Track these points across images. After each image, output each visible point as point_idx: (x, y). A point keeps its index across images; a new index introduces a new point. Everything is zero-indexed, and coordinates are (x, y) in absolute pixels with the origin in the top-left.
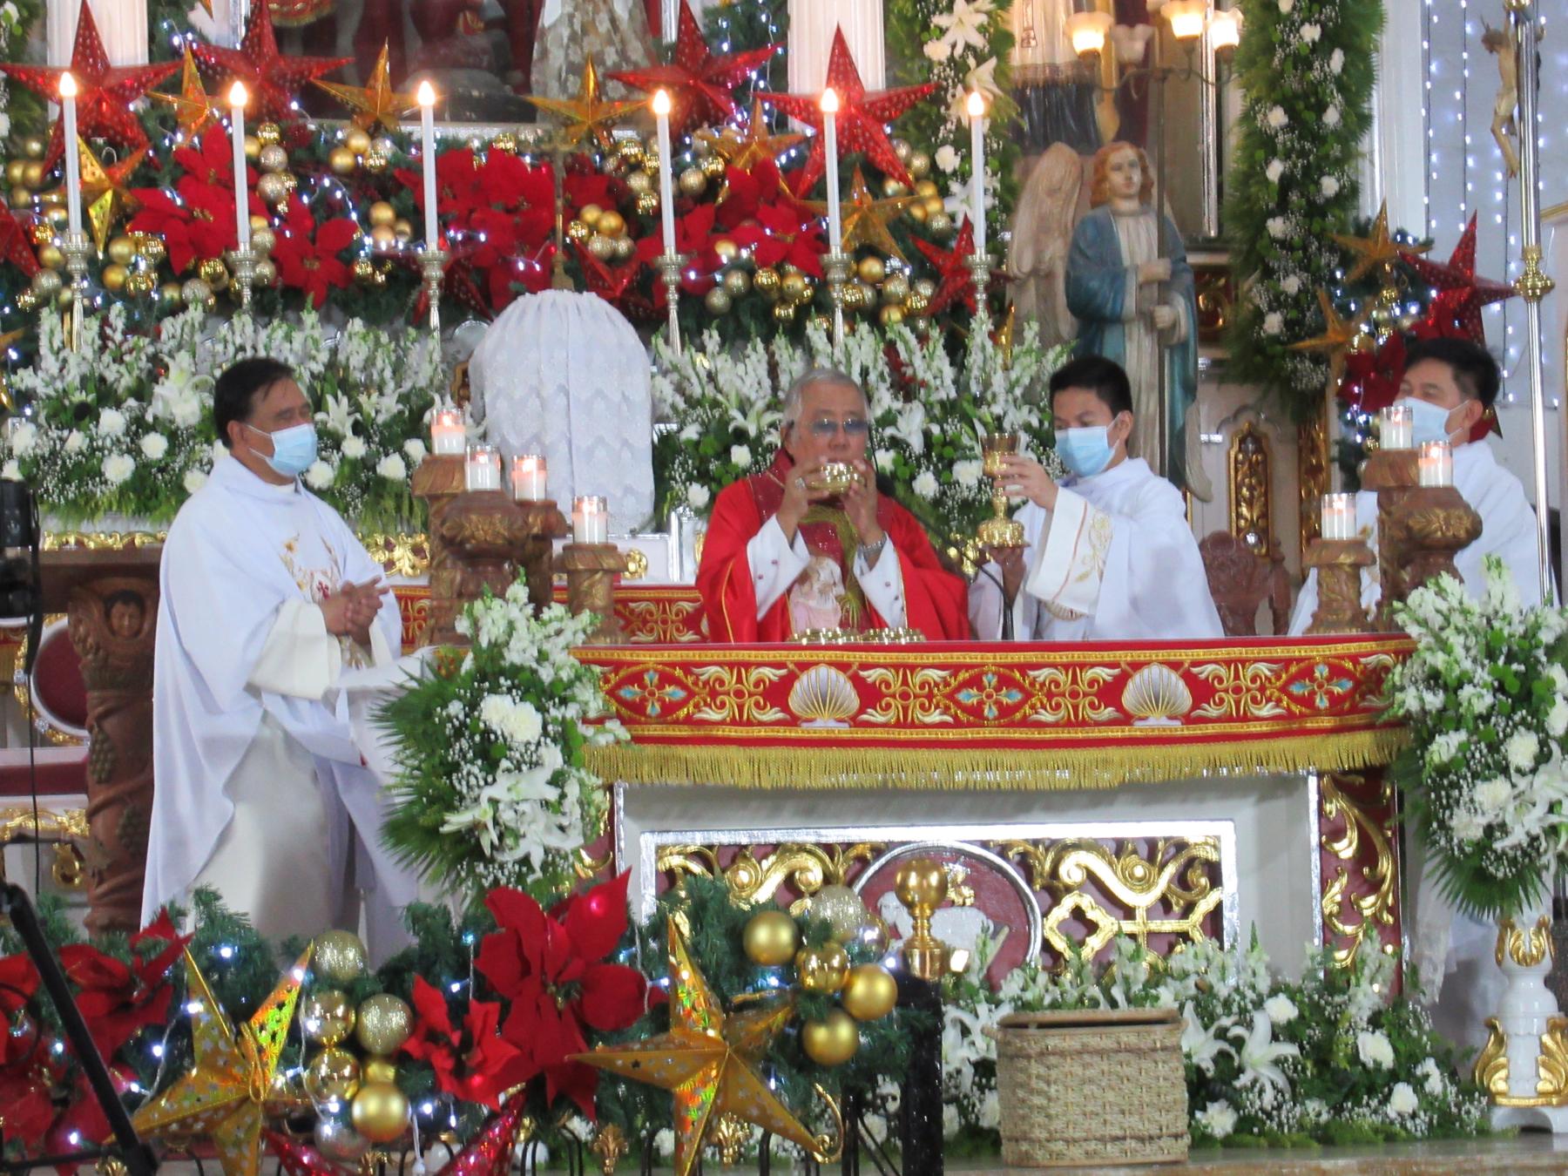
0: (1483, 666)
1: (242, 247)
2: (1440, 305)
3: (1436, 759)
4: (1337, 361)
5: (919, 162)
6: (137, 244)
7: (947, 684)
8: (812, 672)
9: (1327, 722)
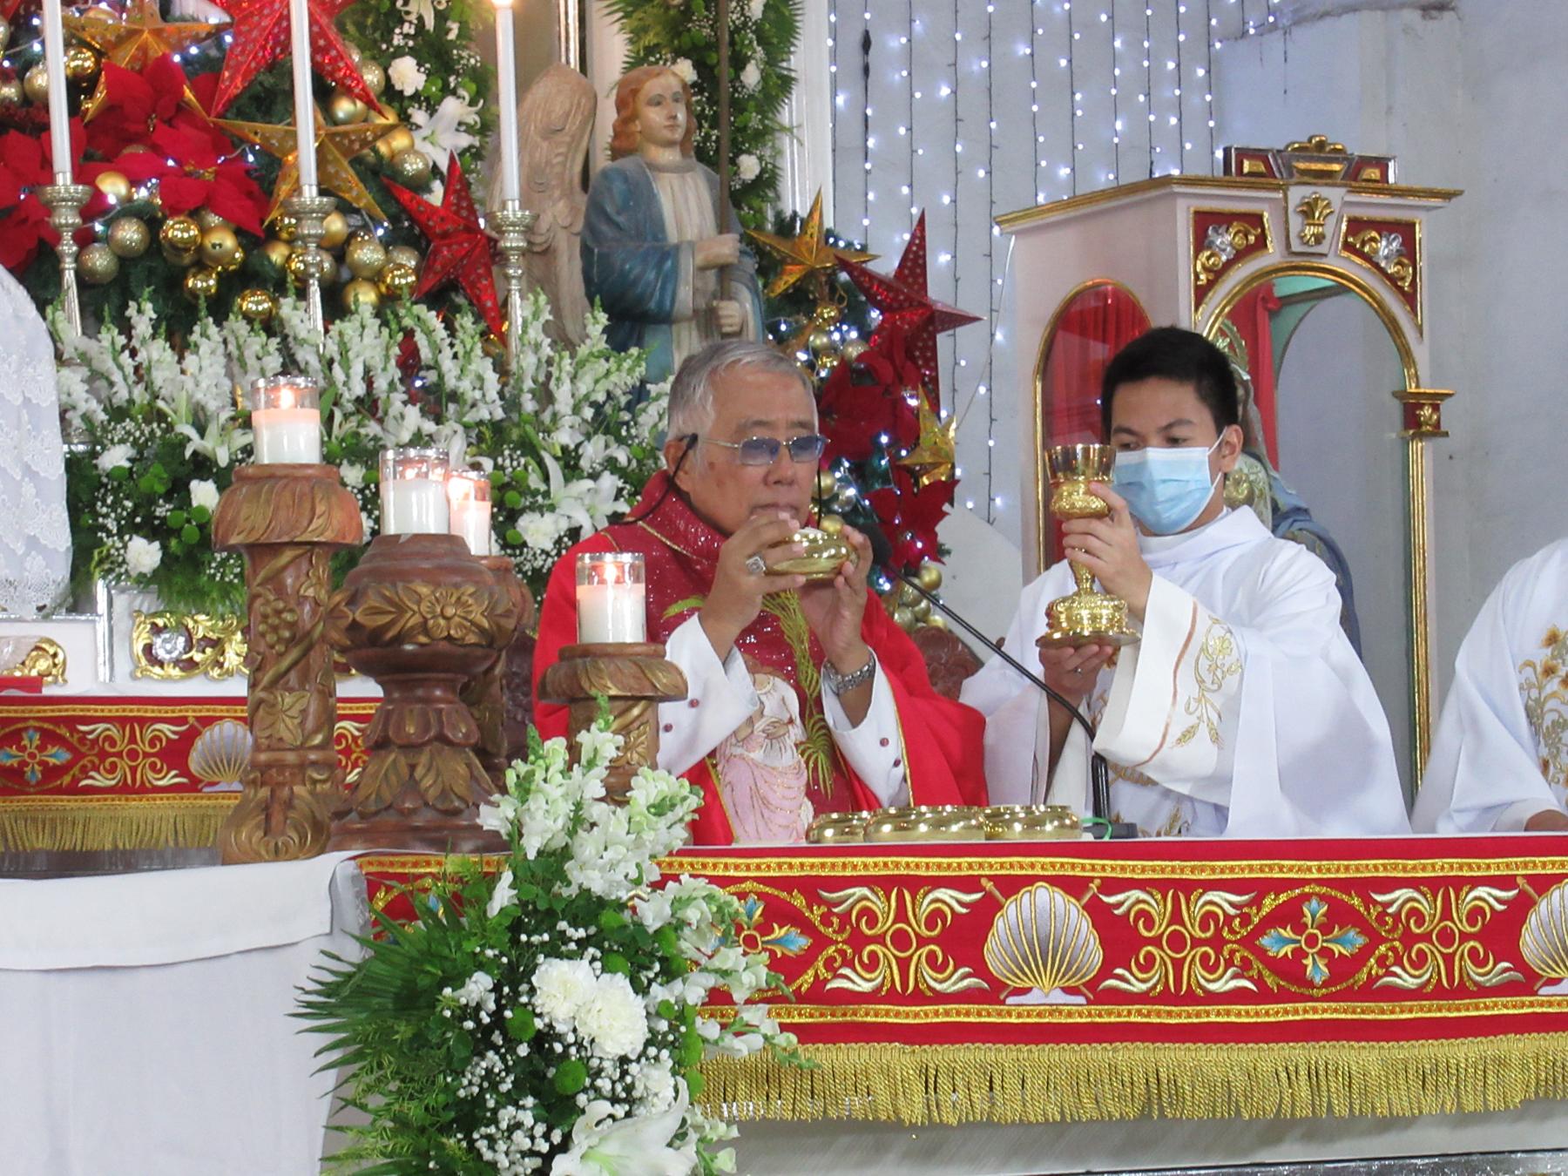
5: (372, 77)
8: (1024, 896)
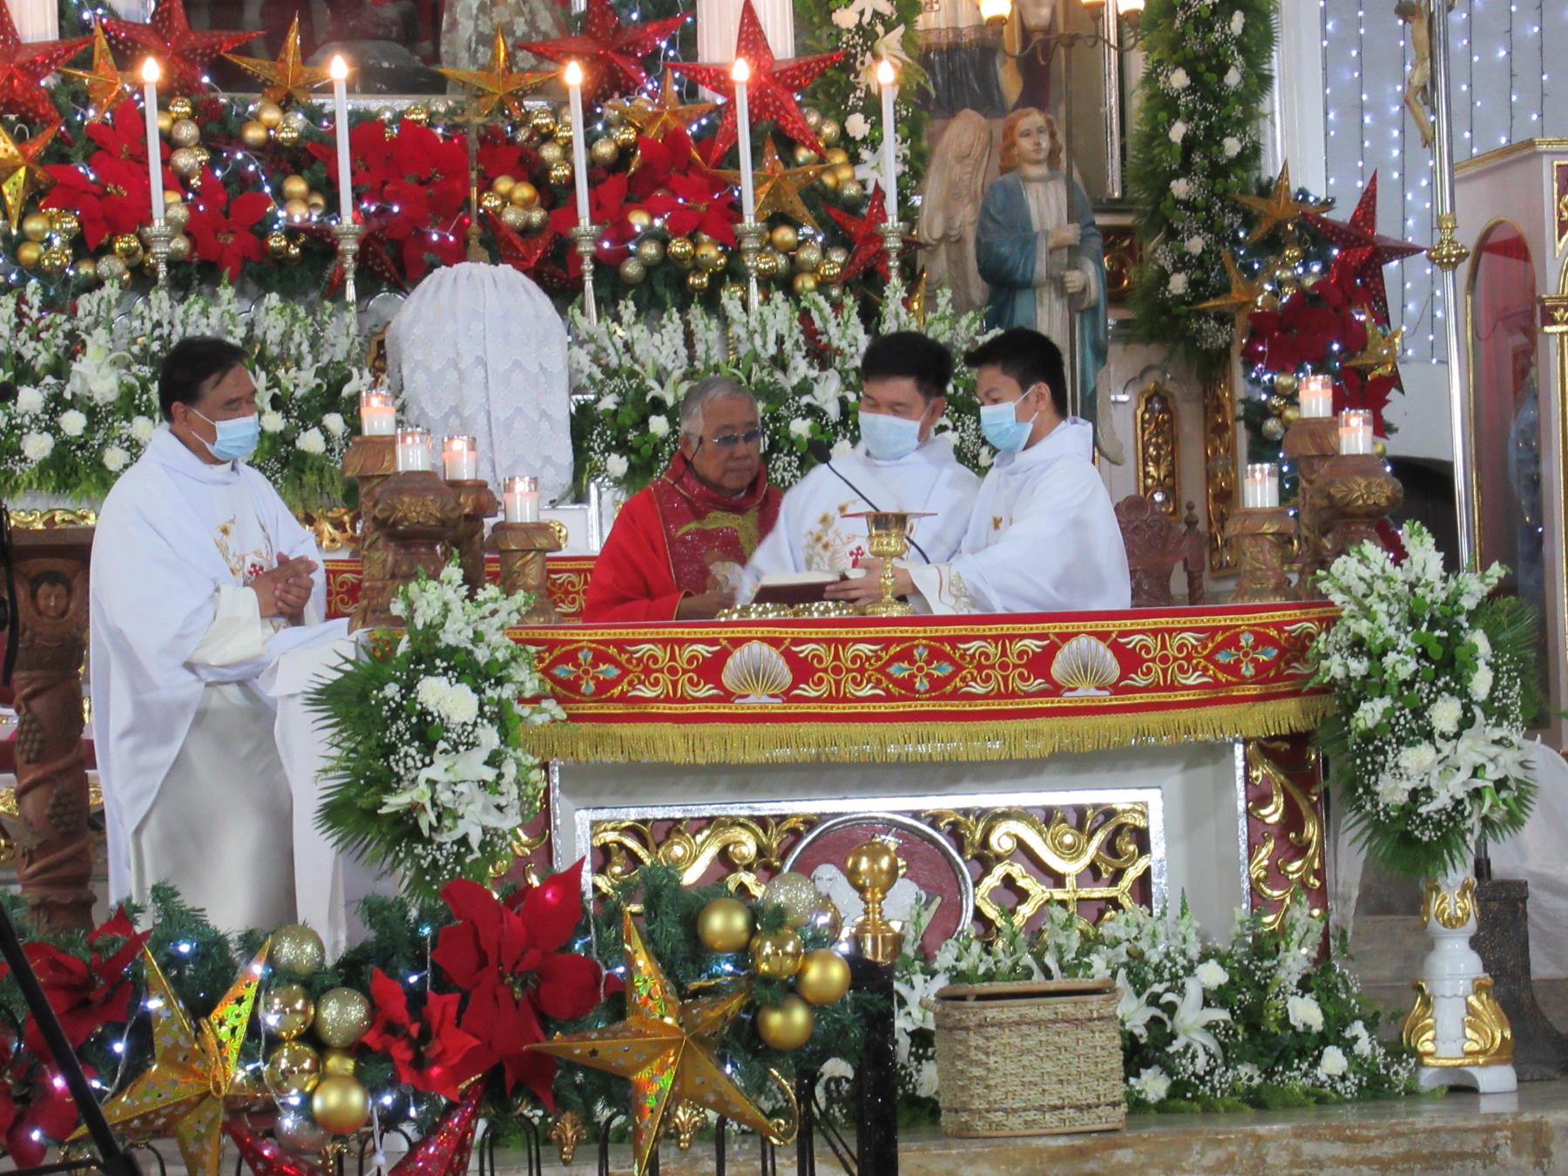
0: (1407, 633)
1: (157, 223)
2: (1341, 263)
3: (1361, 724)
4: (1241, 320)
5: (830, 130)
6: (51, 220)
7: (879, 658)
8: (745, 648)
9: (1253, 690)
